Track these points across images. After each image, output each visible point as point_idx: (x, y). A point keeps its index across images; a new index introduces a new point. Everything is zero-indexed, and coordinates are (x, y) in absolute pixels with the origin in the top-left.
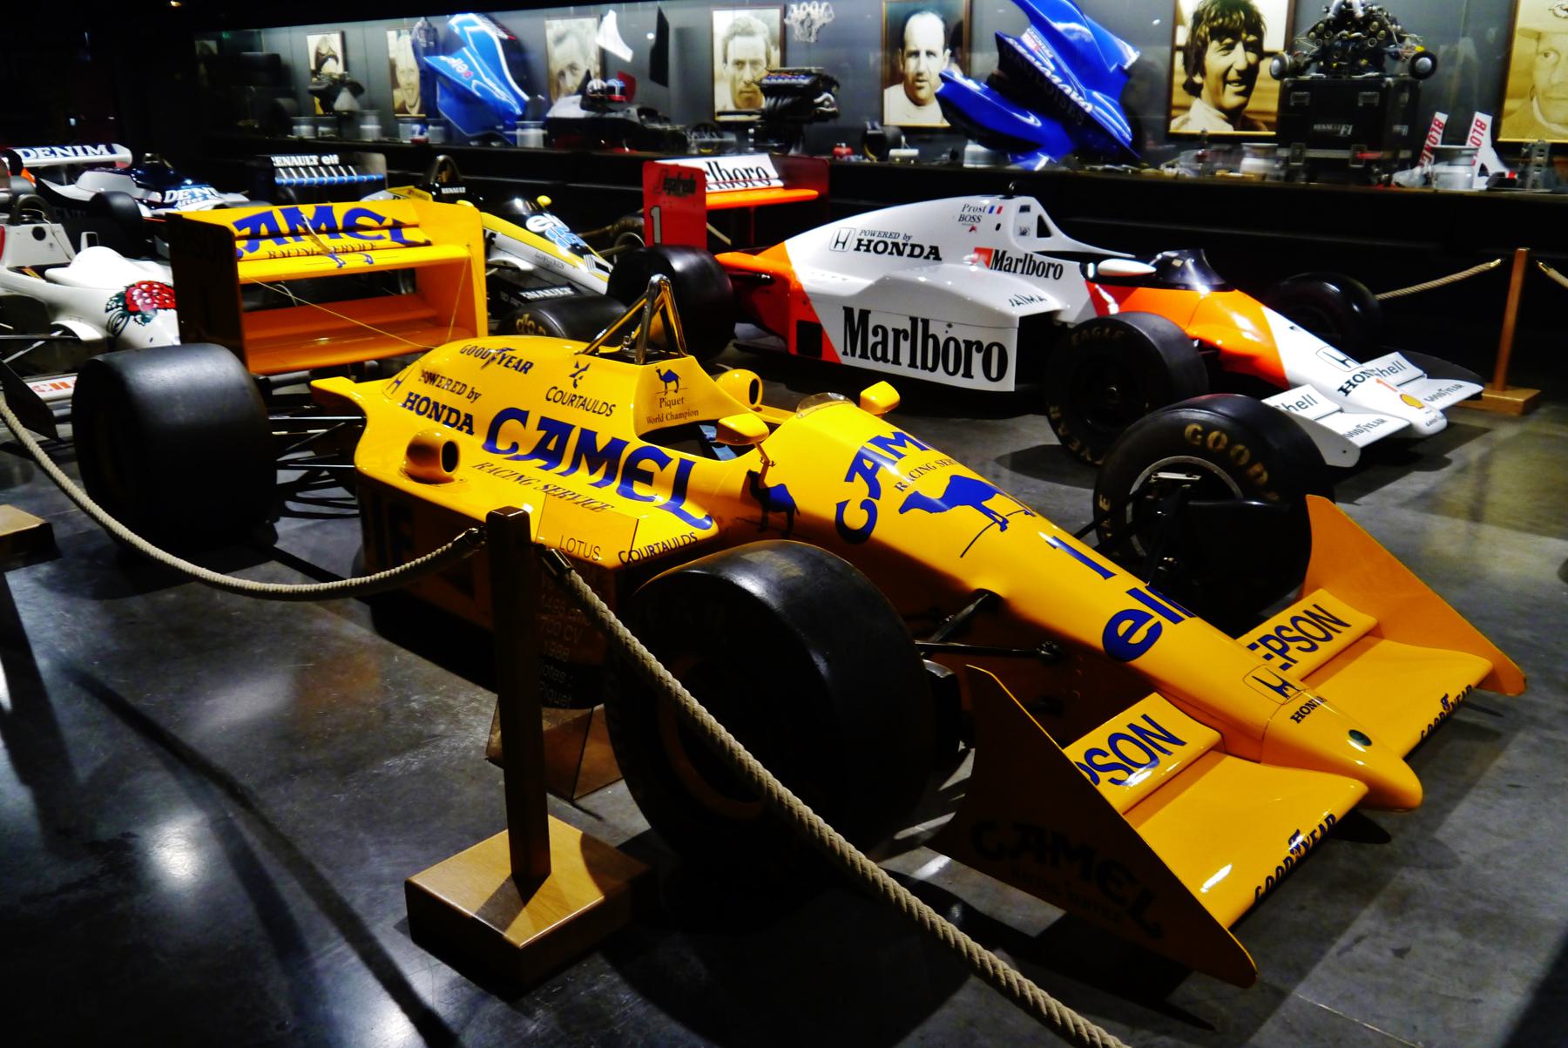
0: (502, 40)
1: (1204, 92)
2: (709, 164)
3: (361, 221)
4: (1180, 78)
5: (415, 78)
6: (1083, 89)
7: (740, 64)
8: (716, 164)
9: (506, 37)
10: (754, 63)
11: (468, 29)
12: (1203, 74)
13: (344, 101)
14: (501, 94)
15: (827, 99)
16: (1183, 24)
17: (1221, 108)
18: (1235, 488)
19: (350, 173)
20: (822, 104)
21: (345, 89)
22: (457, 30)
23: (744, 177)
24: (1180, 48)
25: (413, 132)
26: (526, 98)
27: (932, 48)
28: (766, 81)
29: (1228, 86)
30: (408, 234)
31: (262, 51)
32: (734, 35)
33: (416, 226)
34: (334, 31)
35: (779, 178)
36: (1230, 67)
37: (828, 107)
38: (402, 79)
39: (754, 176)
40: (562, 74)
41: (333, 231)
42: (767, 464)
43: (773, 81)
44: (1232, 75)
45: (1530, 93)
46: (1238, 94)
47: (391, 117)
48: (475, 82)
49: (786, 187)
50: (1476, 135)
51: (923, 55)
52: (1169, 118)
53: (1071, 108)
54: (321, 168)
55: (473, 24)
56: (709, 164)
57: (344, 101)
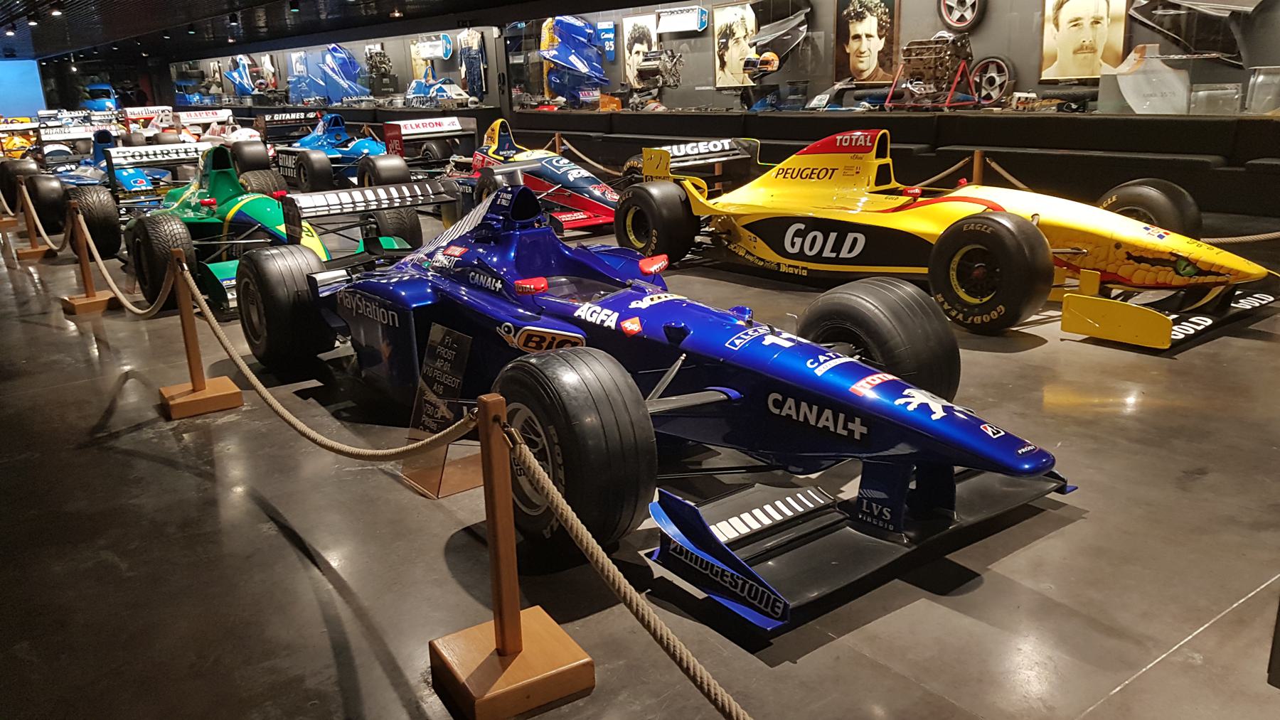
9: (250, 63)
41: (8, 123)
57: (214, 90)
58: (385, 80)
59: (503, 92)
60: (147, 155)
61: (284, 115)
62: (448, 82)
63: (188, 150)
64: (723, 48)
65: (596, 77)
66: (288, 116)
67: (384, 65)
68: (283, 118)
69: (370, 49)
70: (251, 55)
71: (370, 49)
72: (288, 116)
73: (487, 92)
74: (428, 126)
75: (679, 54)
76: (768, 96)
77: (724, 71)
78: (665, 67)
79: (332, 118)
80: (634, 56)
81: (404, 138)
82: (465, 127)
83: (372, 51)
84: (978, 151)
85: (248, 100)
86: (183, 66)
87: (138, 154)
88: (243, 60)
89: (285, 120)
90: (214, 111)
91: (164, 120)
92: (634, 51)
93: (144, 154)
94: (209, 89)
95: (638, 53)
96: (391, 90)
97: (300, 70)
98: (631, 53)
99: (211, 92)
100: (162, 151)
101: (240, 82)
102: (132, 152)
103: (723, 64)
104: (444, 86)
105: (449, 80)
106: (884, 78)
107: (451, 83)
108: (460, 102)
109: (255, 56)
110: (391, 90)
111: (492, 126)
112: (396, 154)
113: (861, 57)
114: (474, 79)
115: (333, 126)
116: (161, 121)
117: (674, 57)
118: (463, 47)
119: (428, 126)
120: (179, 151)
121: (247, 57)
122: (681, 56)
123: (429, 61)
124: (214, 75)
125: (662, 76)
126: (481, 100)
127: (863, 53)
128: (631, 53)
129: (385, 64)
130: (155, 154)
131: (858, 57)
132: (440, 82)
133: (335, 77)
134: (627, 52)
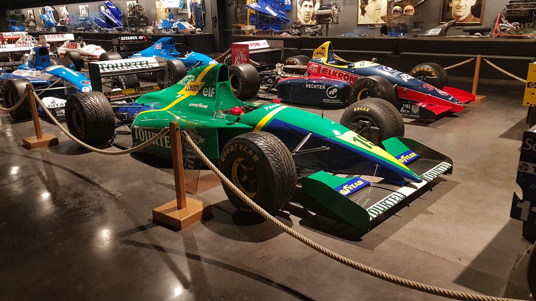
9: (53, 10)
10: (85, 15)
11: (48, 9)
22: (46, 9)
32: (81, 11)
39: (20, 35)
58: (142, 19)
59: (215, 26)
60: (117, 67)
61: (126, 37)
62: (183, 20)
63: (143, 63)
64: (364, 4)
65: (282, 18)
66: (128, 38)
67: (141, 12)
68: (126, 39)
69: (133, 3)
70: (53, 6)
71: (133, 3)
72: (128, 38)
73: (204, 26)
74: (253, 45)
75: (339, 7)
76: (355, 30)
77: (364, 15)
78: (334, 13)
79: (169, 39)
80: (303, 8)
81: (250, 52)
82: (273, 45)
83: (134, 4)
84: (479, 57)
86: (11, 12)
87: (111, 66)
88: (48, 8)
89: (127, 40)
90: (62, 35)
91: (27, 39)
92: (303, 5)
93: (115, 65)
94: (29, 23)
95: (306, 6)
96: (145, 24)
97: (84, 14)
98: (301, 6)
99: (30, 25)
100: (126, 63)
101: (48, 20)
102: (107, 65)
103: (364, 12)
104: (182, 23)
105: (184, 20)
106: (474, 20)
107: (185, 21)
108: (191, 31)
109: (56, 7)
110: (145, 24)
111: (323, 46)
112: (241, 63)
113: (459, 9)
114: (198, 19)
115: (169, 44)
116: (26, 40)
117: (337, 8)
118: (193, 2)
119: (253, 45)
120: (137, 63)
122: (340, 7)
123: (167, 10)
124: (30, 16)
125: (332, 18)
126: (202, 29)
127: (461, 7)
128: (301, 6)
129: (142, 11)
130: (122, 66)
131: (458, 9)
132: (179, 21)
133: (110, 18)
134: (299, 6)
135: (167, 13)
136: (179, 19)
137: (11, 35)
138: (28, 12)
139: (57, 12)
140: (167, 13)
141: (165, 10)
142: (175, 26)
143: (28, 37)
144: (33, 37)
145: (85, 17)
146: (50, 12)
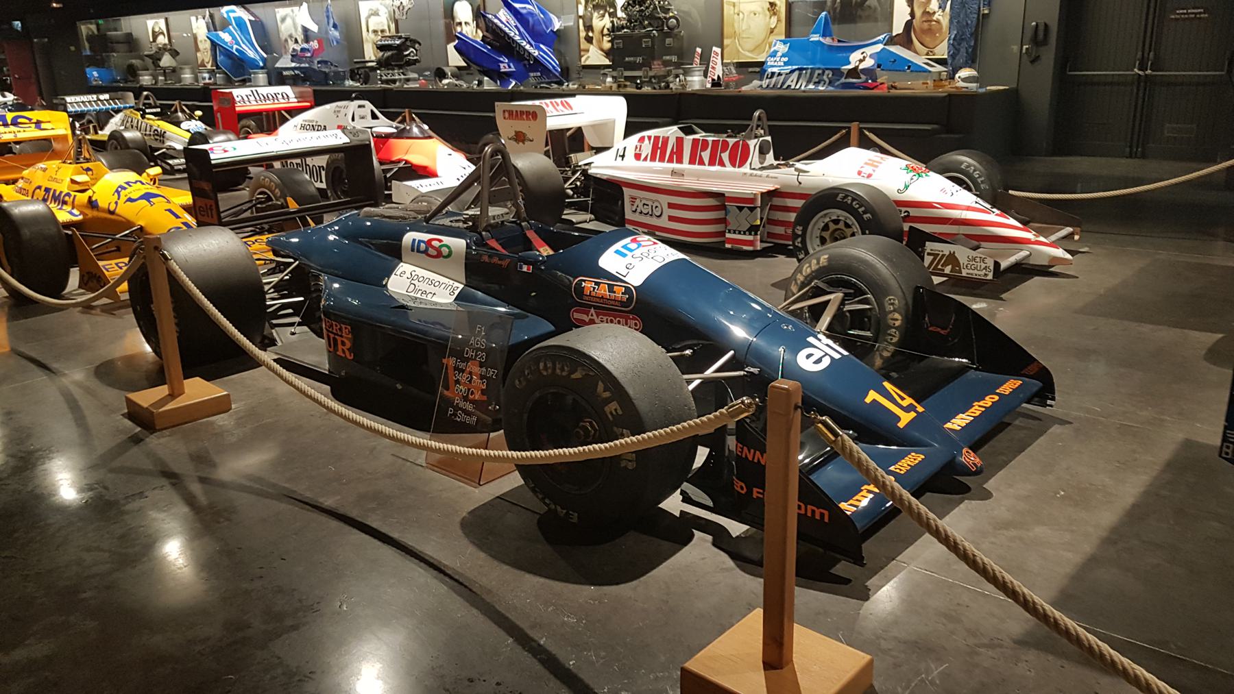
0: (250, 20)
1: (594, 41)
2: (252, 91)
3: (20, 120)
4: (583, 34)
5: (208, 45)
6: (533, 43)
7: (375, 32)
8: (256, 91)
9: (253, 19)
10: (382, 31)
11: (232, 15)
12: (593, 31)
13: (166, 61)
14: (251, 54)
15: (412, 52)
16: (581, 3)
17: (602, 50)
18: (273, 198)
19: (116, 104)
20: (409, 55)
21: (166, 53)
22: (225, 16)
23: (273, 97)
24: (580, 17)
25: (204, 79)
26: (265, 56)
27: (467, 21)
28: (379, 43)
29: (604, 38)
30: (43, 126)
31: (122, 31)
32: (369, 17)
33: (49, 122)
34: (161, 17)
35: (296, 98)
36: (604, 27)
37: (413, 56)
38: (201, 46)
39: (280, 97)
40: (286, 41)
42: (94, 192)
43: (383, 43)
44: (606, 32)
45: (734, 35)
46: (609, 41)
47: (197, 67)
48: (235, 46)
49: (298, 102)
50: (714, 59)
51: (463, 24)
52: (581, 57)
53: (526, 54)
54: (99, 102)
55: (234, 11)
56: (252, 91)
57: (166, 61)
85: (261, 75)
90: (563, 100)
91: (356, 117)
94: (160, 60)
109: (260, 10)
121: (242, 9)
135: (774, 19)
136: (881, 37)
137: (252, 98)
138: (150, 26)
139: (261, 21)
140: (774, 19)
141: (768, 6)
142: (861, 61)
143: (360, 106)
144: (376, 108)
145: (400, 38)
146: (240, 23)
